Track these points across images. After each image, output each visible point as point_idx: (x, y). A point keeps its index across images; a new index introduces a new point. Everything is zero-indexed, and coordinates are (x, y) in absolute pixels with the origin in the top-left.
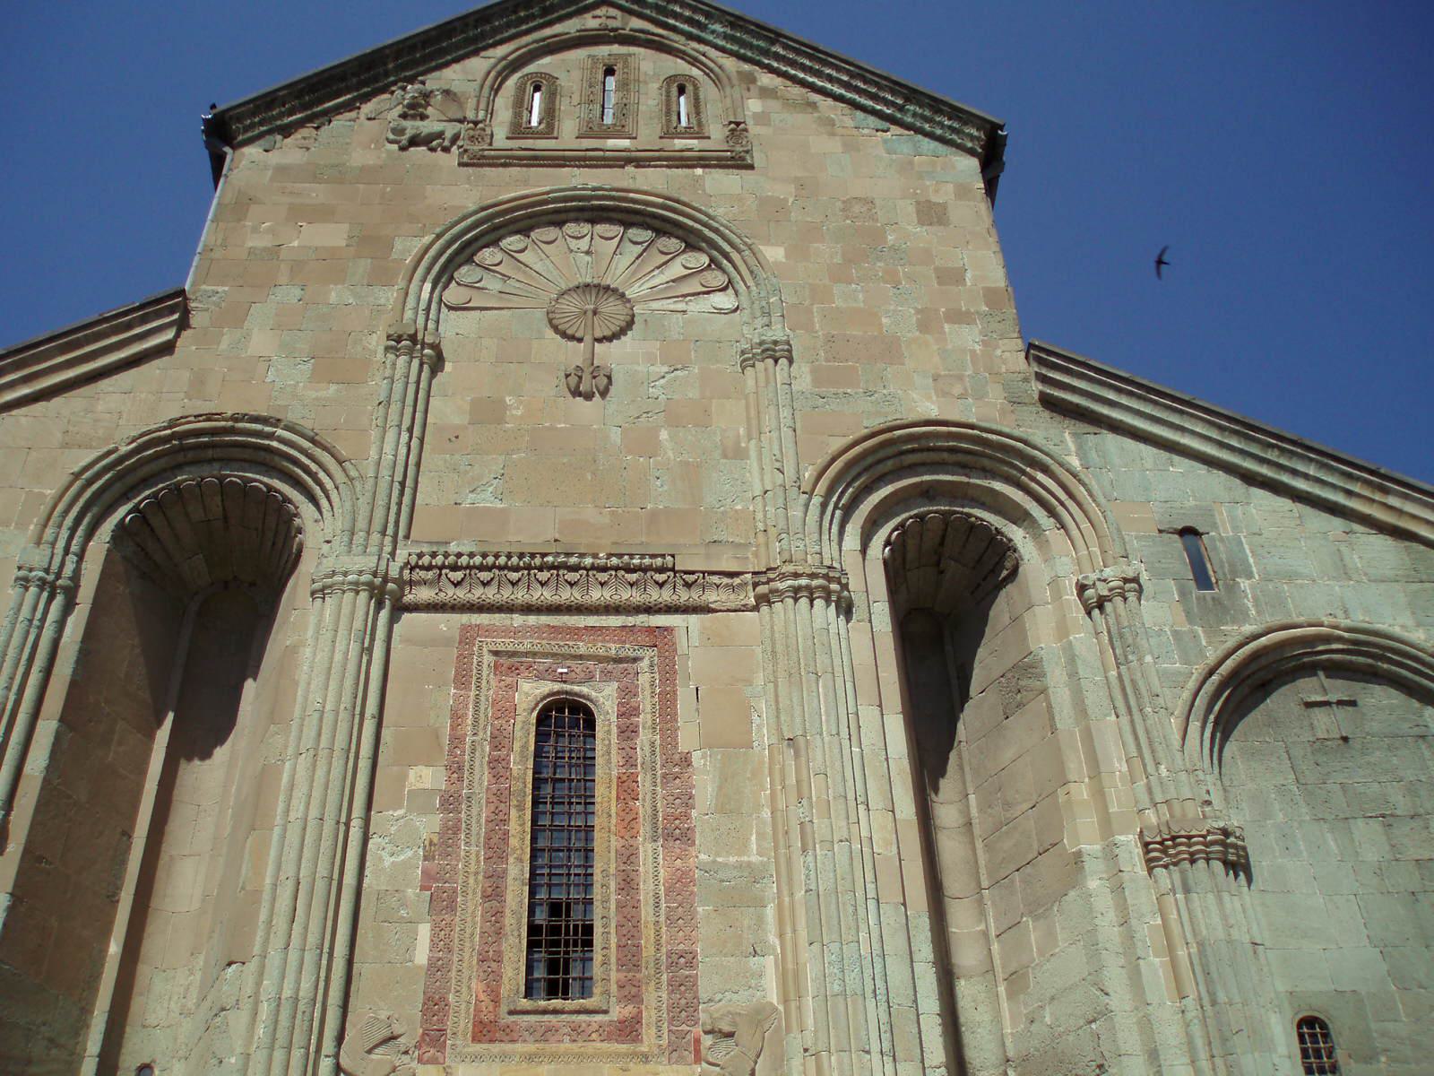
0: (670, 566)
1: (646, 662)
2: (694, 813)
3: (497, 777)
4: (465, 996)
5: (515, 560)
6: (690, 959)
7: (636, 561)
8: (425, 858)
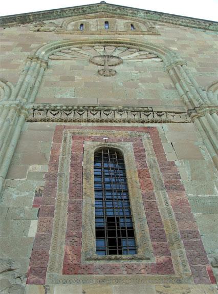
1: (145, 136)
5: (81, 108)
8: (36, 195)
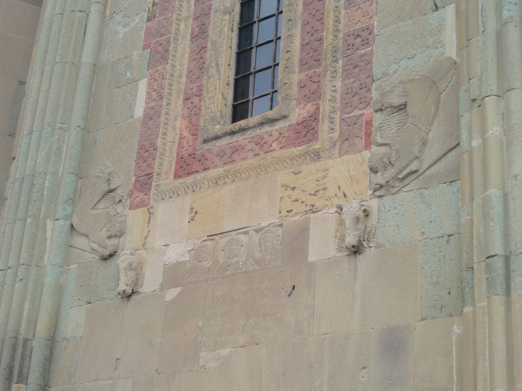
4: (171, 135)
8: (149, 19)
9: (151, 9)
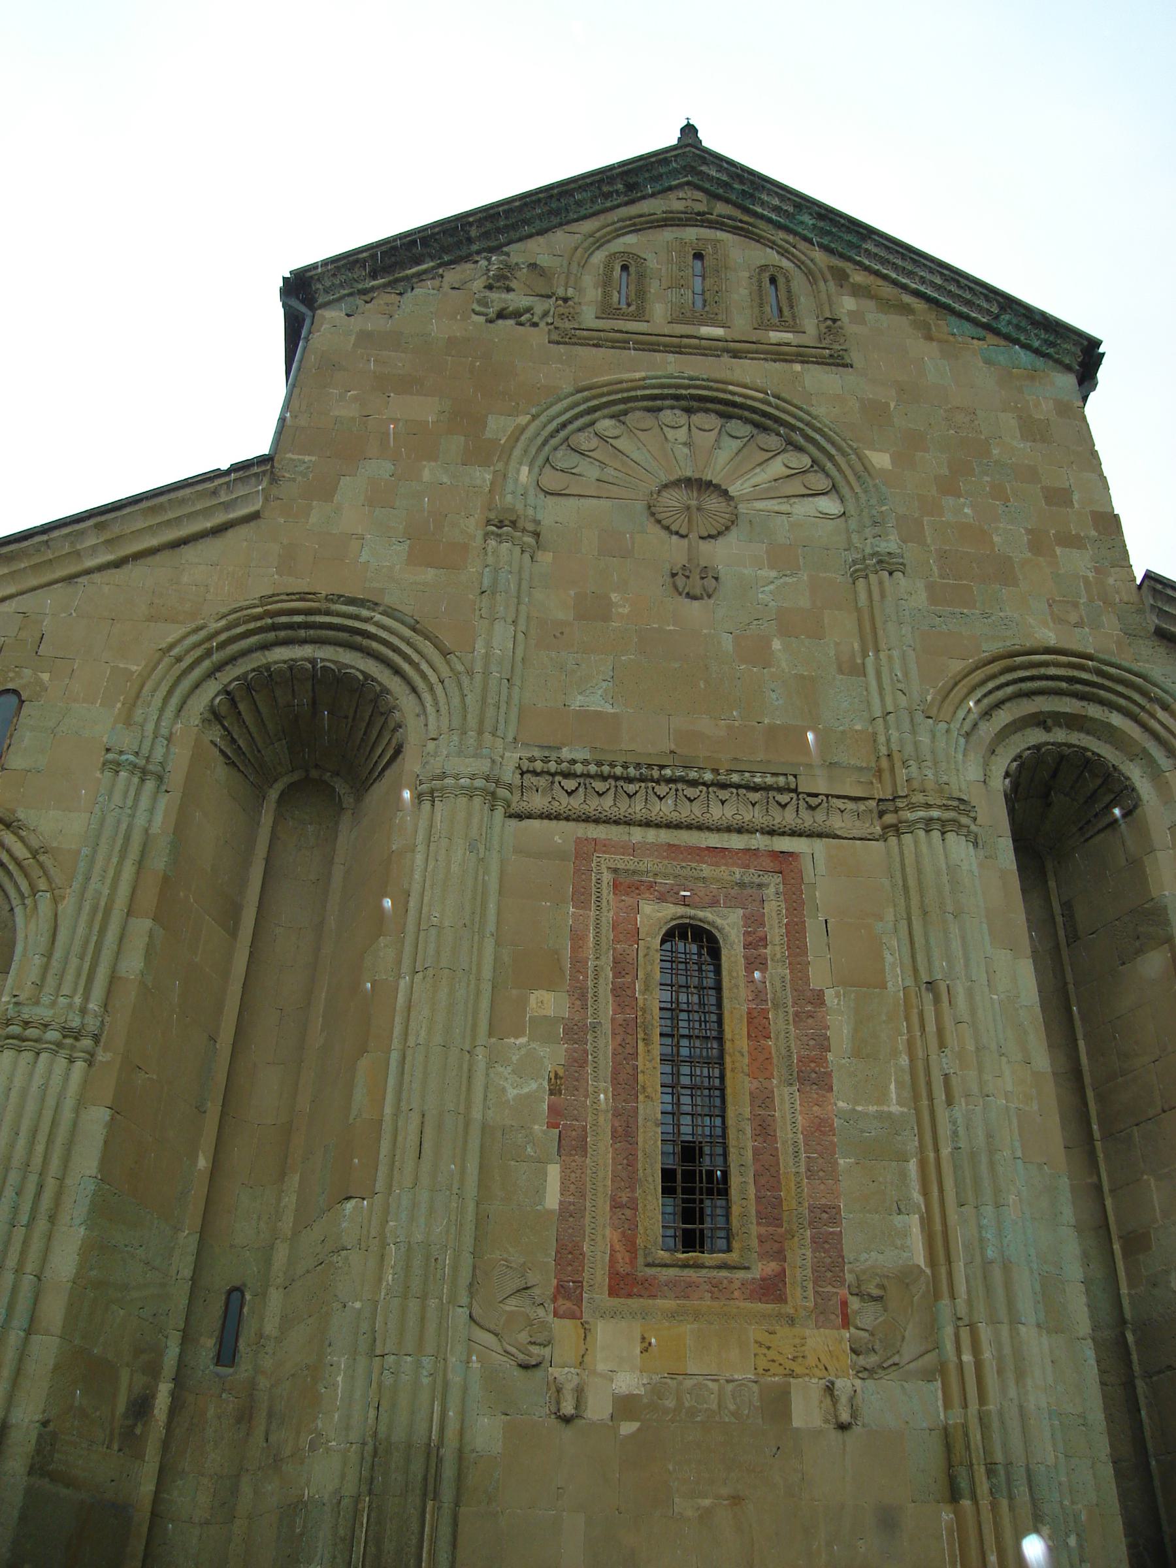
0: (793, 786)
1: (771, 890)
2: (830, 1056)
3: (620, 1006)
5: (632, 771)
6: (831, 1213)
7: (758, 780)
8: (551, 1093)
9: (553, 1080)
